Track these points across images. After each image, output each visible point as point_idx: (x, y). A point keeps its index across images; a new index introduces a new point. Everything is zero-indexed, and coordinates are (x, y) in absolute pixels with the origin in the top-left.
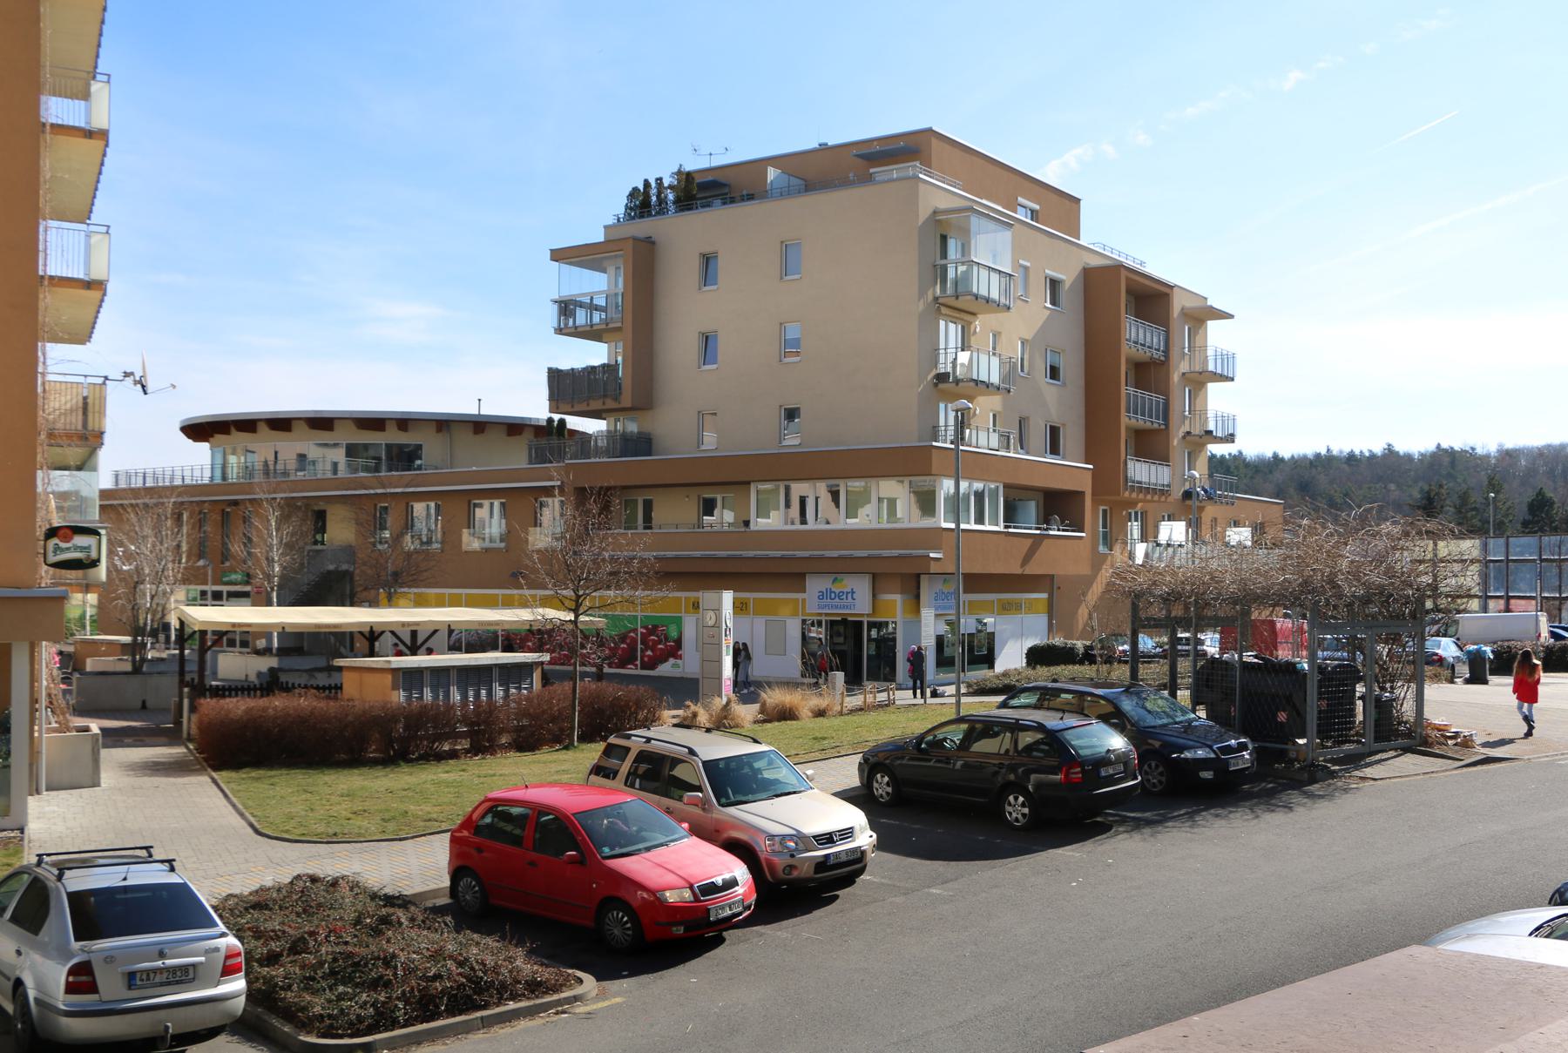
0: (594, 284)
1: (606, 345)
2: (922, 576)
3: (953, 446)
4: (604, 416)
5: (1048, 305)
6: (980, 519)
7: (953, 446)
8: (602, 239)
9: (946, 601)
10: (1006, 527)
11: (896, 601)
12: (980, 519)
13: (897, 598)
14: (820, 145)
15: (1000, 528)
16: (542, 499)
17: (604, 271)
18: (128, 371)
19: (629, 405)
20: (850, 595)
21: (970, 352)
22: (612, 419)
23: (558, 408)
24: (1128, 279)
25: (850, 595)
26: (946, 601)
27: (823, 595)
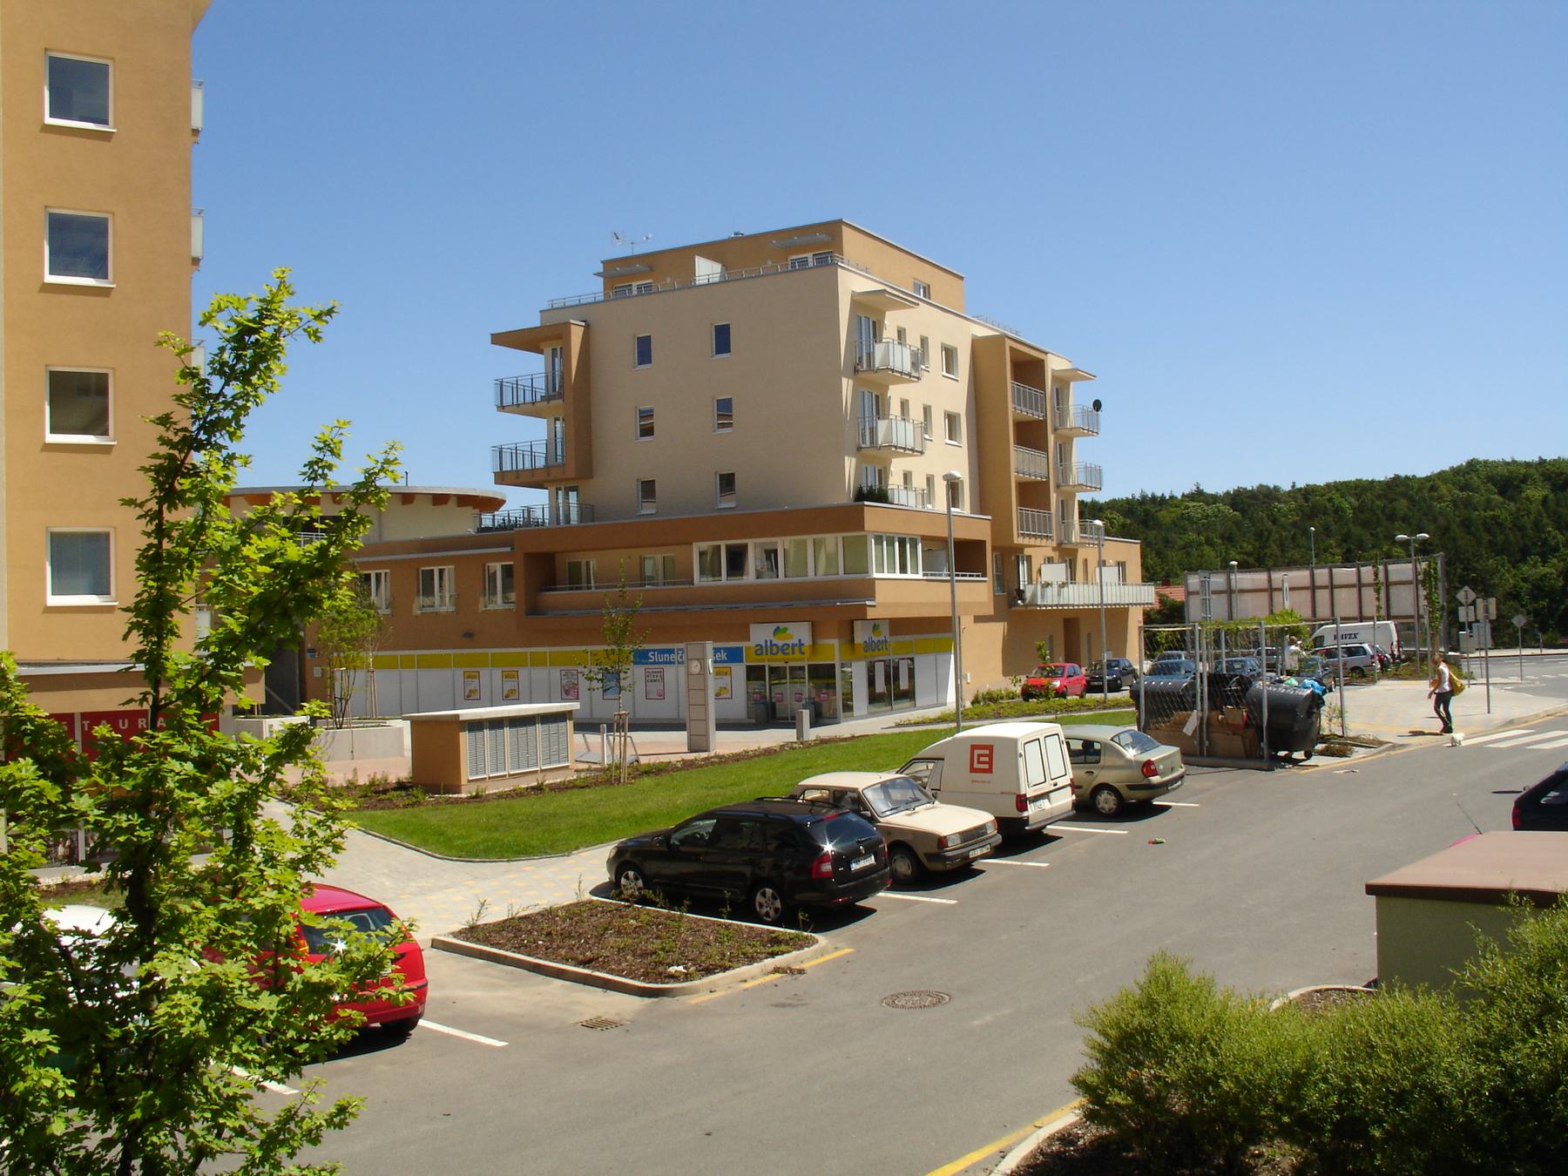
0: (531, 367)
1: (545, 420)
2: (855, 622)
3: (949, 578)
4: (545, 485)
5: (944, 373)
6: (903, 569)
7: (949, 578)
8: (539, 325)
9: (877, 651)
10: (924, 575)
11: (833, 645)
12: (903, 569)
13: (835, 642)
14: (736, 234)
15: (920, 576)
16: (490, 564)
17: (541, 352)
18: (178, 394)
19: (573, 475)
20: (797, 648)
21: (887, 421)
22: (554, 489)
23: (503, 480)
24: (1012, 349)
25: (797, 648)
26: (877, 651)
27: (761, 649)
